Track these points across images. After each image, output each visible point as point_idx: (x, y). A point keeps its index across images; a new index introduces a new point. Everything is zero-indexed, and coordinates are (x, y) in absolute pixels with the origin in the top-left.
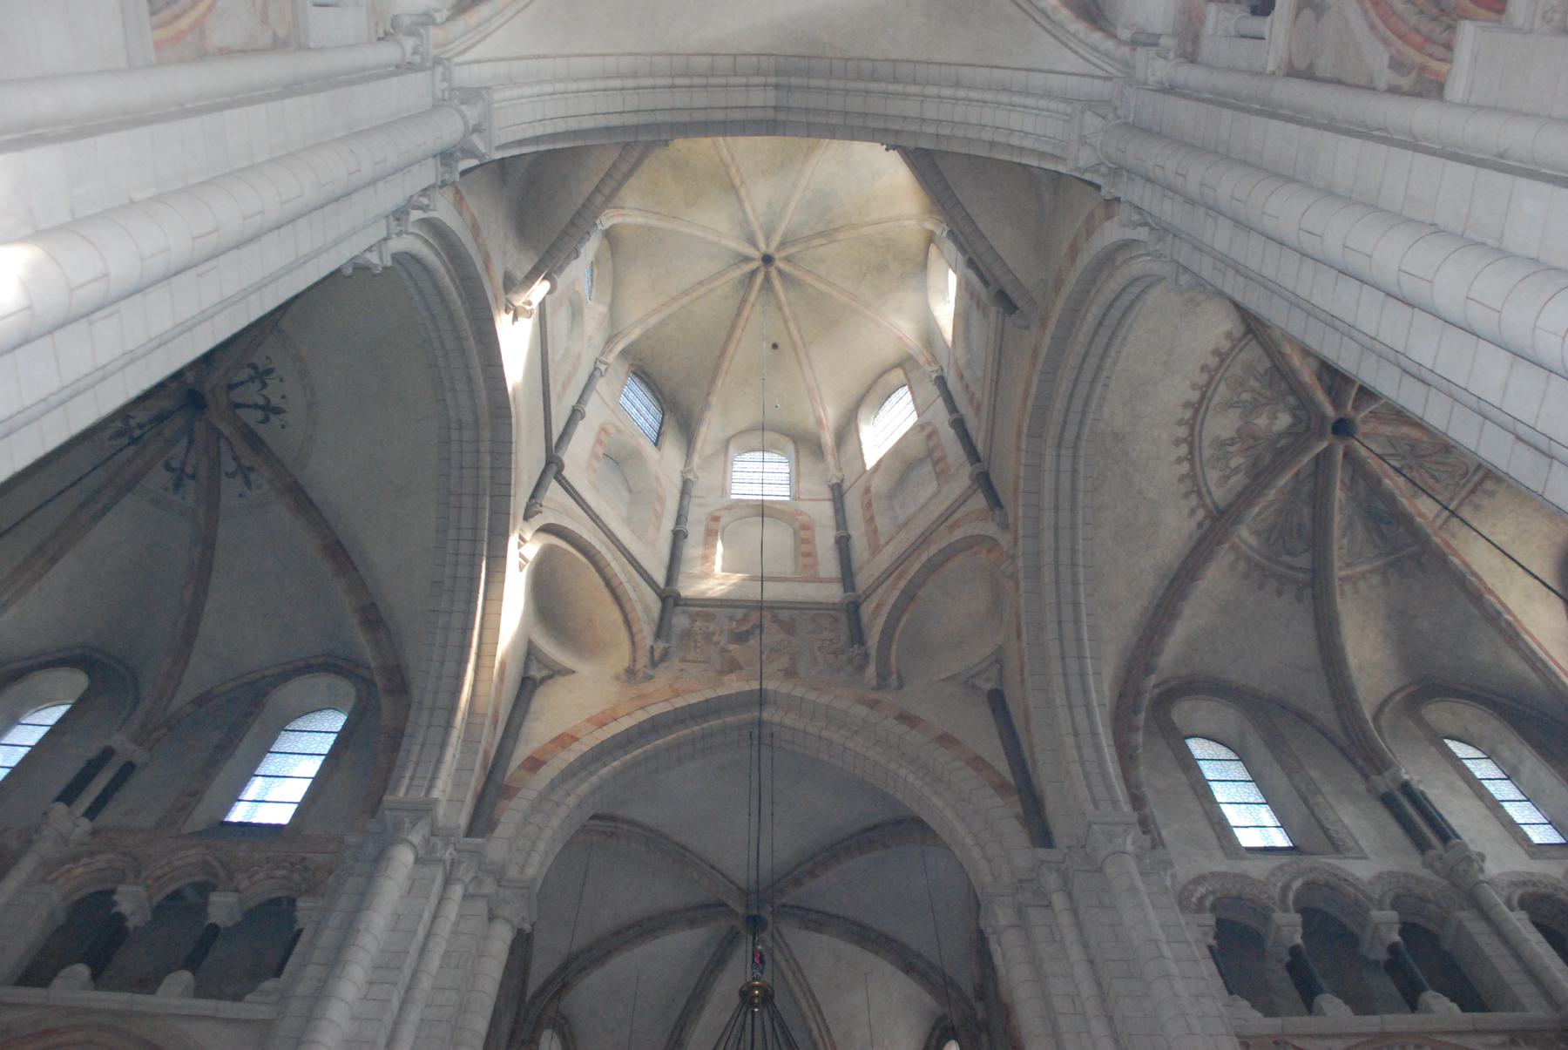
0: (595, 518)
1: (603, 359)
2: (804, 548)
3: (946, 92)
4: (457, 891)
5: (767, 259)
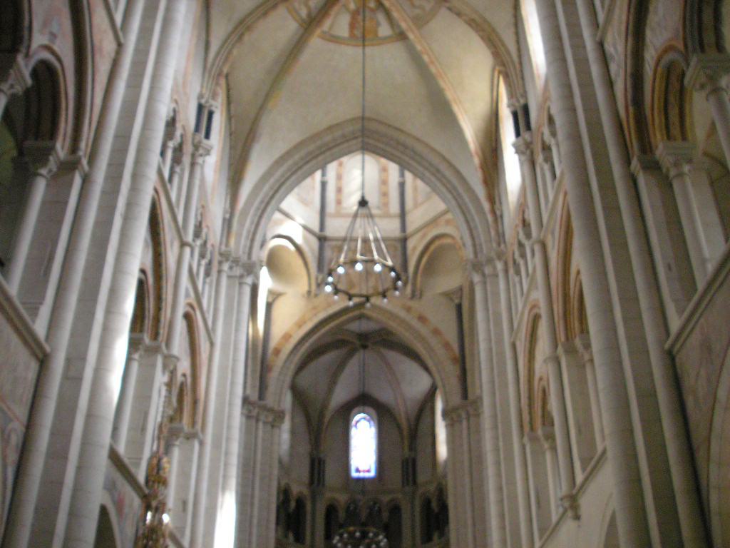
4: (261, 425)
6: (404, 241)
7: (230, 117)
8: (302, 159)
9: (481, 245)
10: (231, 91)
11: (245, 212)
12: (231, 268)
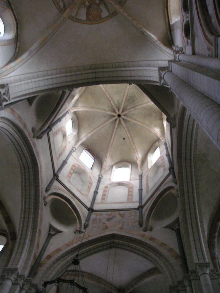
0: (68, 190)
1: (74, 147)
2: (130, 194)
3: (110, 70)
5: (119, 116)
10: (19, 37)
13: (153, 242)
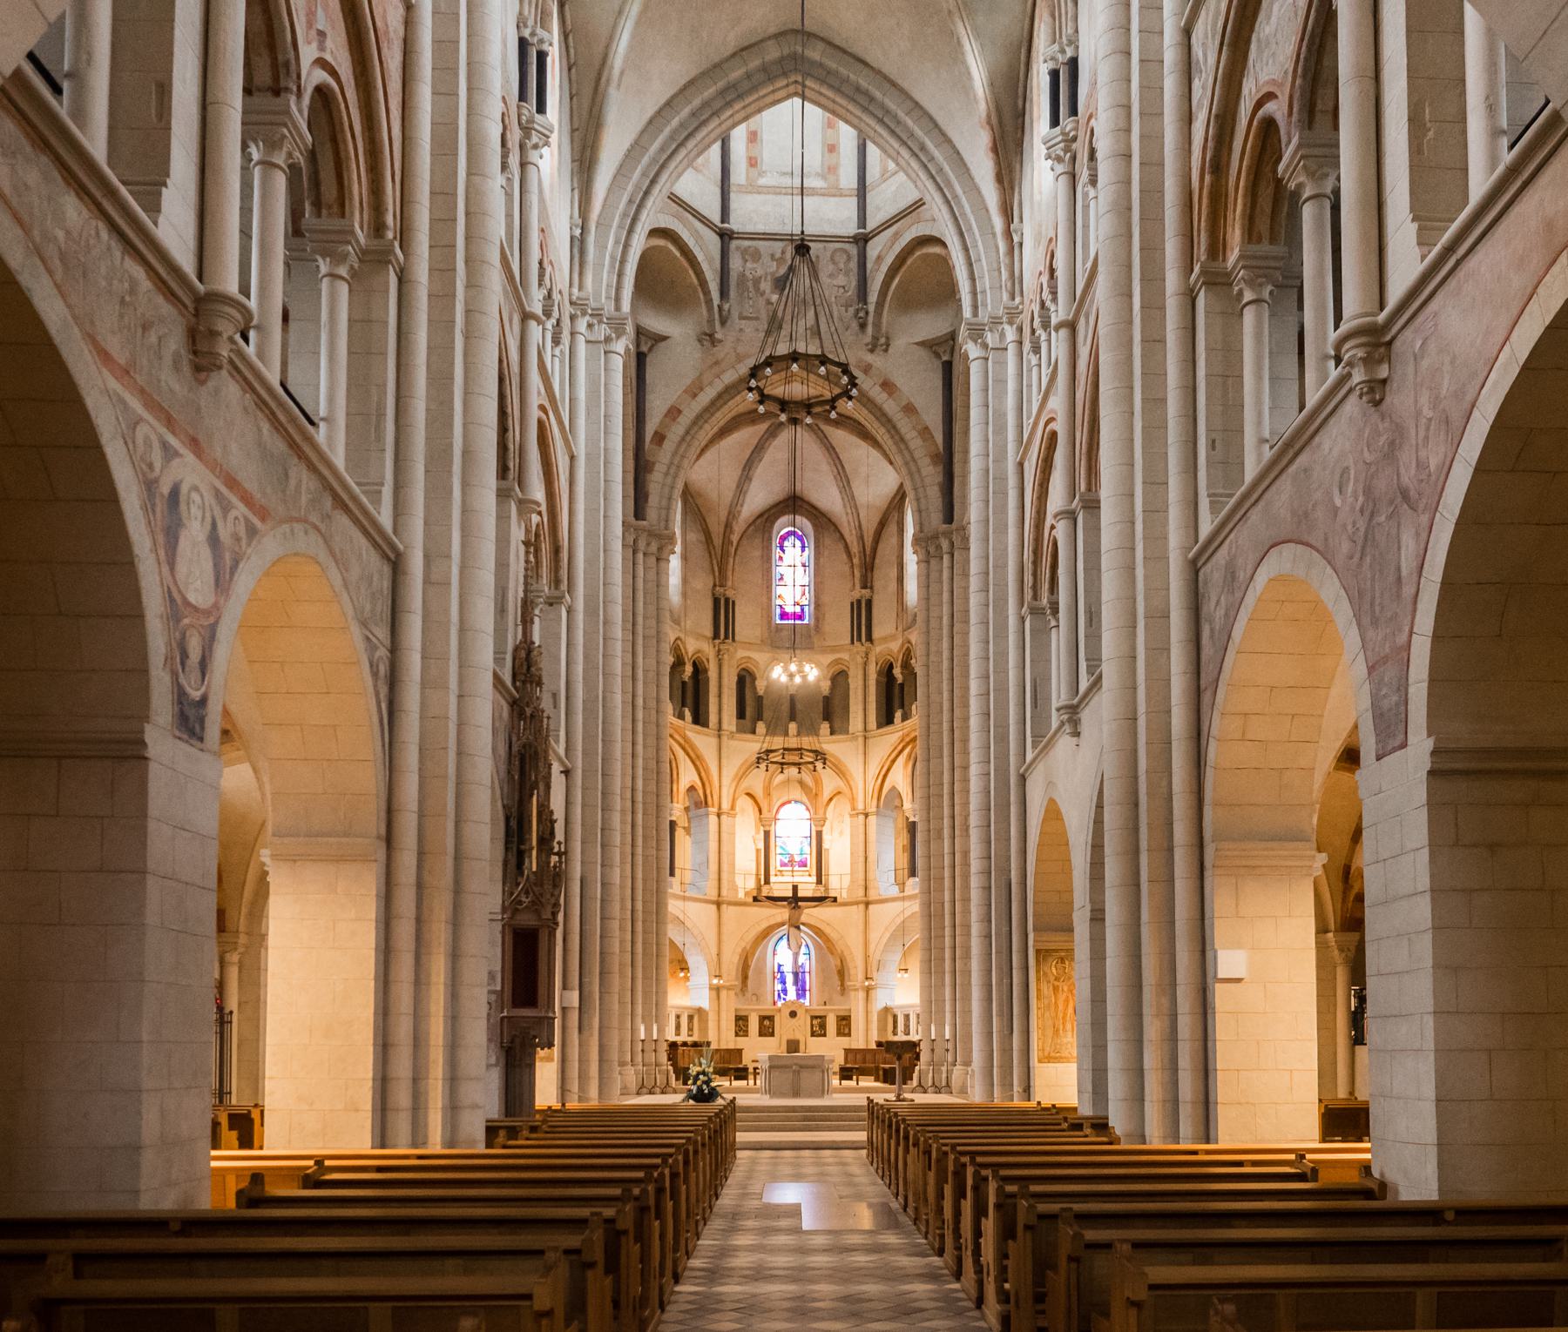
4: (640, 556)
6: (862, 240)
7: (570, 66)
8: (693, 114)
9: (984, 292)
11: (603, 225)
12: (590, 326)
13: (890, 394)
